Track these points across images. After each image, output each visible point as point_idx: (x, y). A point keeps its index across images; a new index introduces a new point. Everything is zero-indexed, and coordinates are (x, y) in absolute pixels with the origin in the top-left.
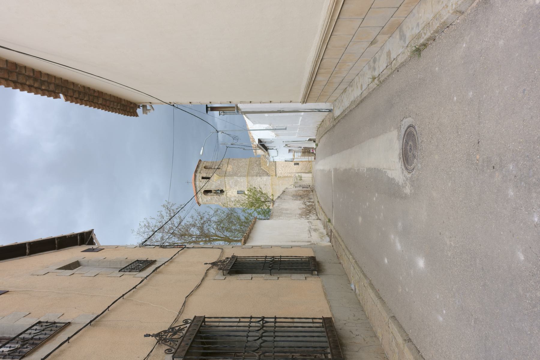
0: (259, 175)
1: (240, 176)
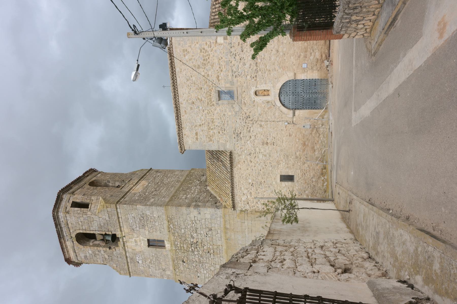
0: (196, 203)
1: (152, 205)
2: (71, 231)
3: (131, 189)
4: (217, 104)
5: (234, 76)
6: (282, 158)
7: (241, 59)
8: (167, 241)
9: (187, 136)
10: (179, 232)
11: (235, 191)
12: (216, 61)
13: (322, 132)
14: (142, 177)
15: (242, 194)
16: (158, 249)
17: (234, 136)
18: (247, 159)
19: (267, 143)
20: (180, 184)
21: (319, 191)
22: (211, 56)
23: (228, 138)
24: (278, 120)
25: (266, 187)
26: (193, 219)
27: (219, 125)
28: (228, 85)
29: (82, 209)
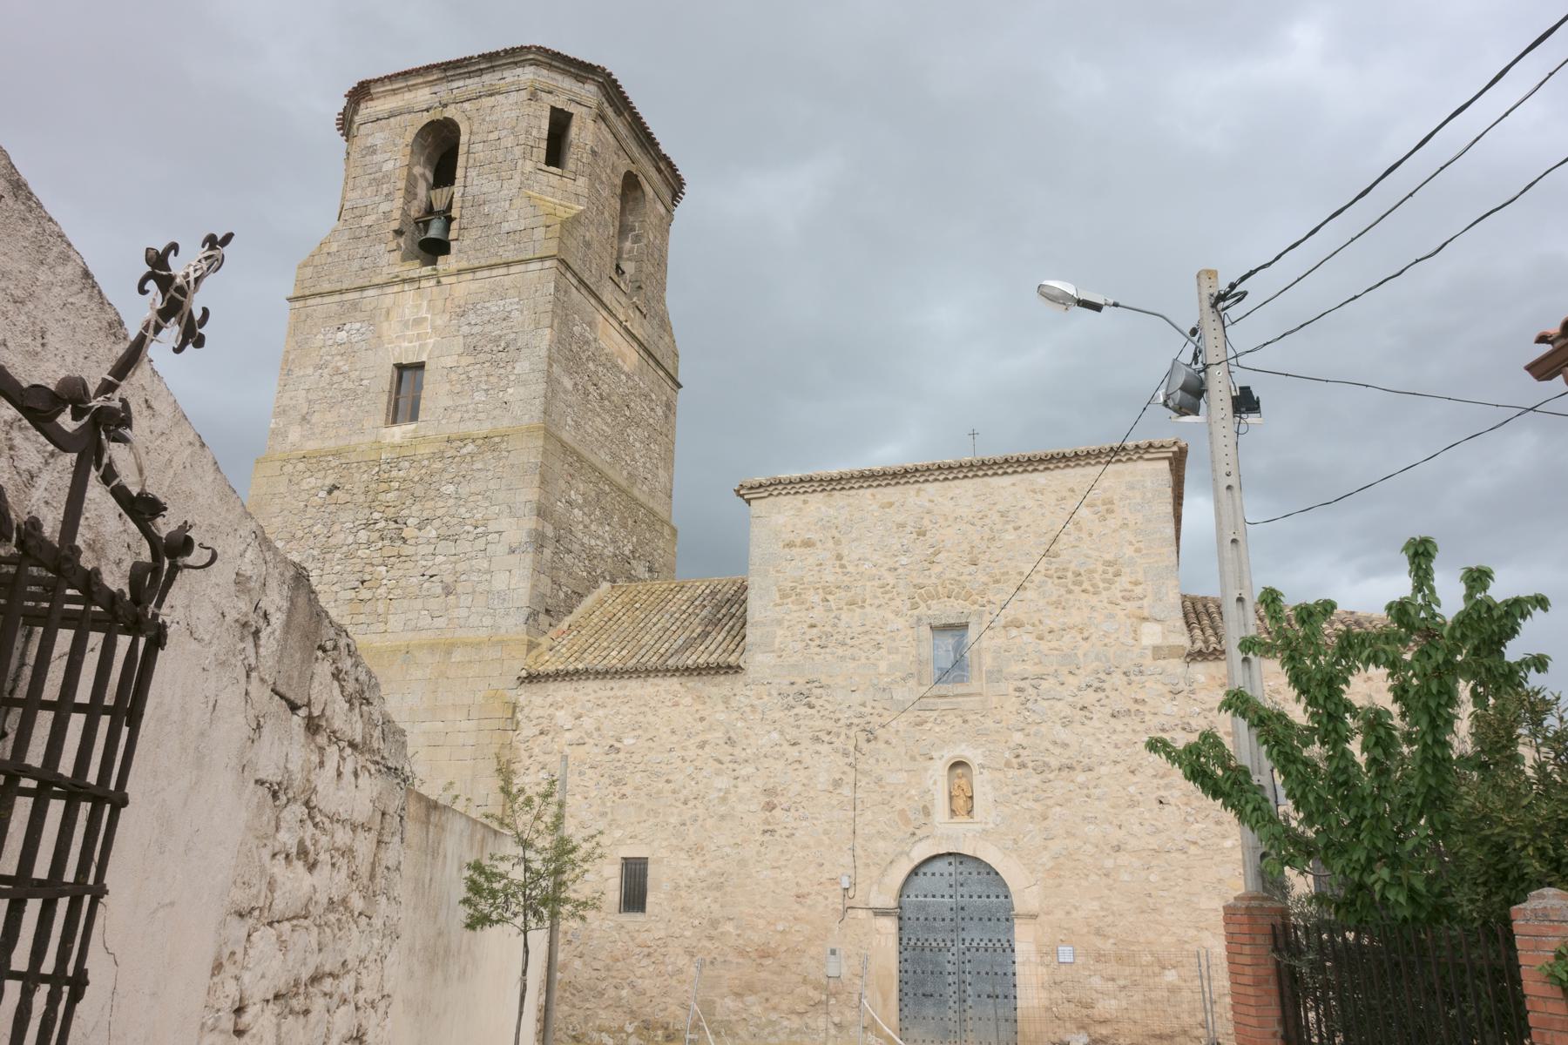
0: (550, 538)
1: (551, 380)
2: (466, 105)
3: (610, 312)
4: (919, 619)
5: (1022, 684)
6: (712, 866)
7: (1083, 708)
8: (414, 431)
9: (800, 510)
10: (446, 476)
11: (592, 685)
12: (1076, 618)
13: (813, 1025)
14: (650, 355)
15: (578, 710)
16: (385, 398)
17: (800, 681)
18: (711, 729)
19: (770, 807)
20: (624, 484)
21: (580, 1013)
22: (1094, 600)
23: (792, 660)
24: (859, 851)
25: (604, 803)
26: (492, 527)
27: (842, 624)
28: (988, 661)
29: (544, 145)
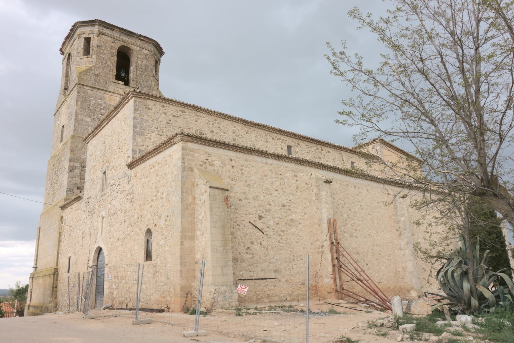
29: (82, 50)
